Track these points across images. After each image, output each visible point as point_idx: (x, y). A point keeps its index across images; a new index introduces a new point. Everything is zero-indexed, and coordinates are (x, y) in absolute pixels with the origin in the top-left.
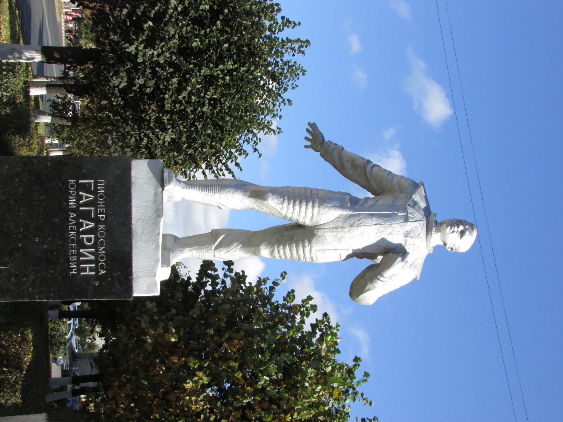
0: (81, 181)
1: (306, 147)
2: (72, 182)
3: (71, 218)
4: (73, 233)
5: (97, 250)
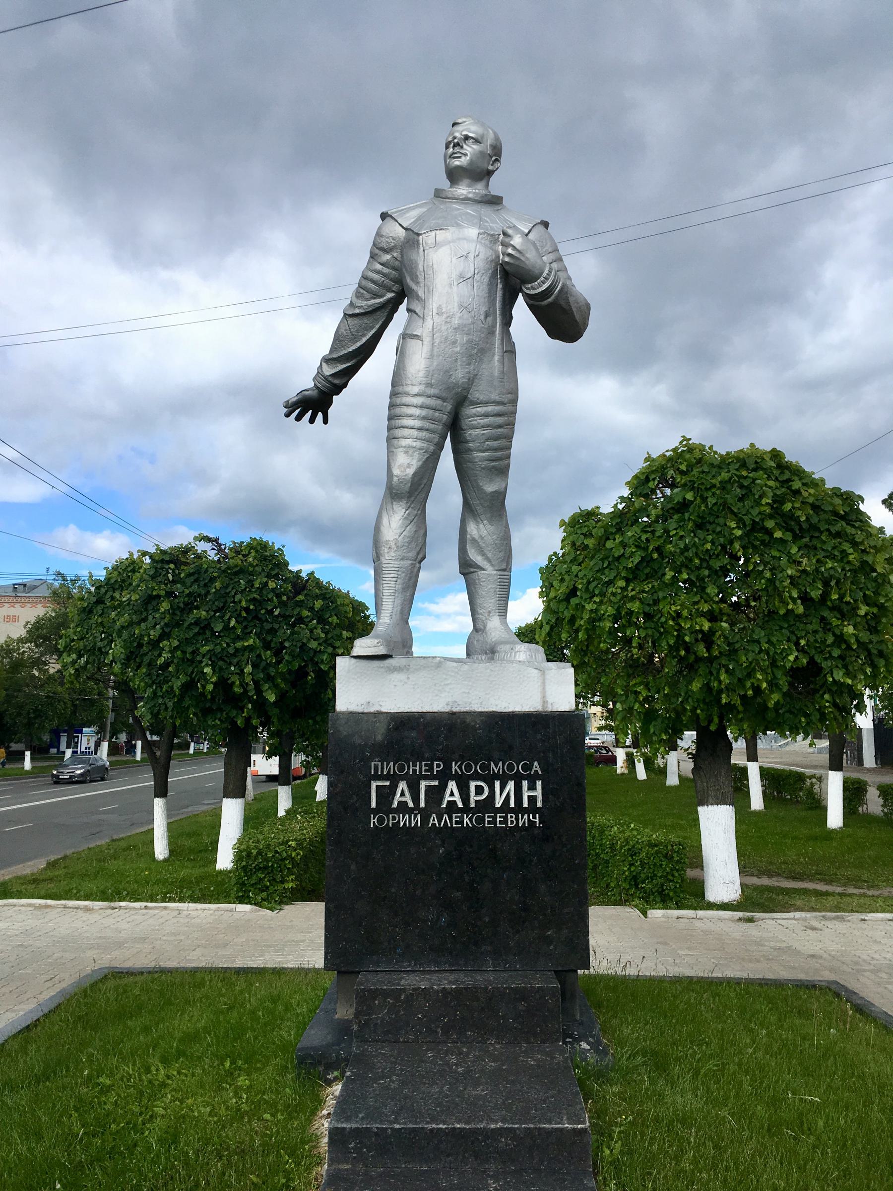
0: (374, 805)
1: (325, 421)
2: (374, 821)
3: (440, 823)
4: (466, 820)
5: (496, 776)
